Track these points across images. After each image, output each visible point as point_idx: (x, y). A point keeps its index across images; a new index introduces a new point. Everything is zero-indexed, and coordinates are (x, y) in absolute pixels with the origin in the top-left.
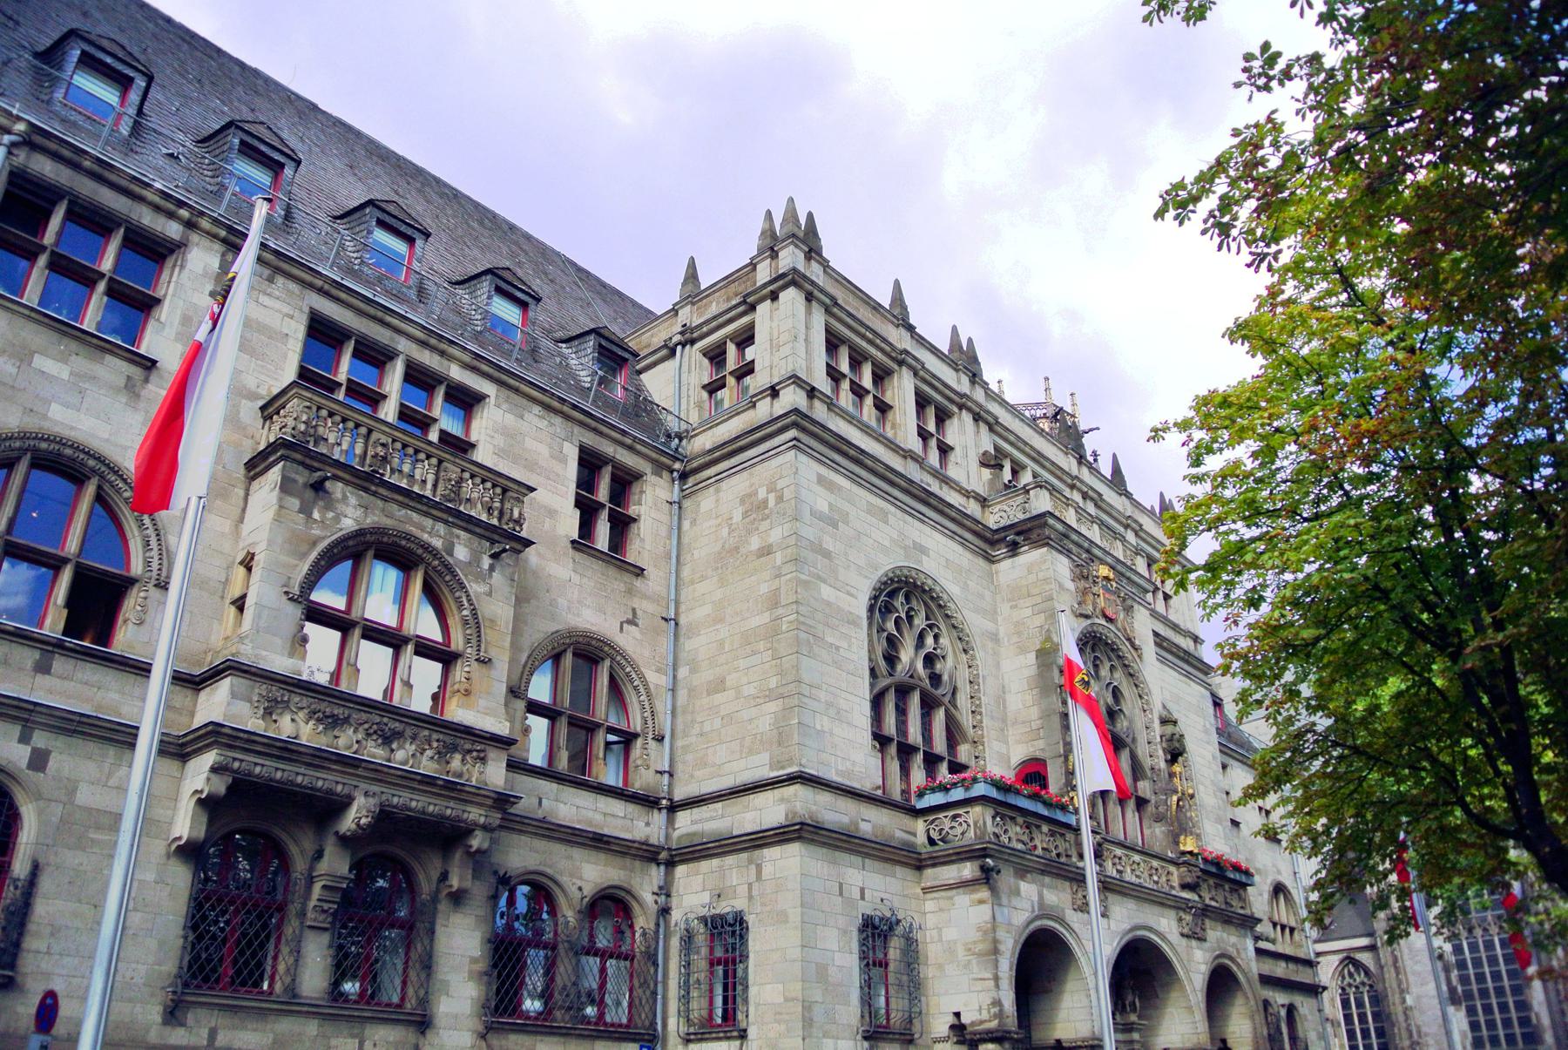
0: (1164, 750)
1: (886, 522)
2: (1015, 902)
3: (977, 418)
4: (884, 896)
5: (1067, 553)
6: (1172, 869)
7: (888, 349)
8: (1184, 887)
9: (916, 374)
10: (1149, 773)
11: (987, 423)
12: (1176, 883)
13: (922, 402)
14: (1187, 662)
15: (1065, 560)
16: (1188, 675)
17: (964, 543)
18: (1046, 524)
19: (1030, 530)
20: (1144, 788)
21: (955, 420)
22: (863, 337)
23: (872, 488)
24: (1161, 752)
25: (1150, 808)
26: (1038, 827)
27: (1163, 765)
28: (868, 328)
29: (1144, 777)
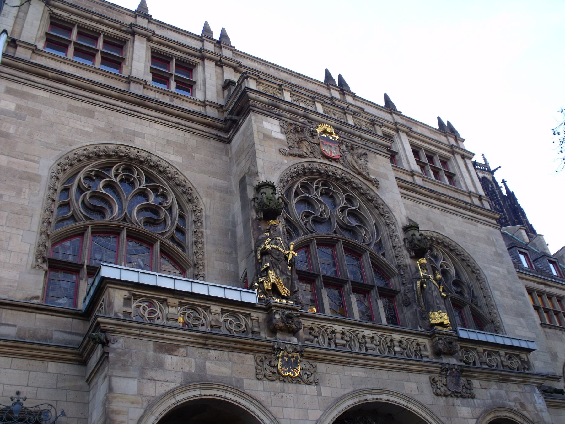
0: (408, 249)
1: (93, 117)
2: (158, 375)
3: (220, 64)
4: (18, 389)
5: (278, 117)
6: (421, 340)
7: (117, 25)
9: (149, 40)
10: (396, 270)
11: (231, 67)
12: (428, 352)
13: (158, 58)
14: (470, 210)
15: (277, 122)
16: (473, 219)
17: (190, 130)
18: (249, 98)
19: (242, 108)
20: (395, 283)
21: (199, 68)
22: (91, 19)
23: (74, 97)
24: (405, 252)
25: (399, 298)
26: (207, 308)
27: (409, 261)
28: (92, 13)
29: (393, 274)
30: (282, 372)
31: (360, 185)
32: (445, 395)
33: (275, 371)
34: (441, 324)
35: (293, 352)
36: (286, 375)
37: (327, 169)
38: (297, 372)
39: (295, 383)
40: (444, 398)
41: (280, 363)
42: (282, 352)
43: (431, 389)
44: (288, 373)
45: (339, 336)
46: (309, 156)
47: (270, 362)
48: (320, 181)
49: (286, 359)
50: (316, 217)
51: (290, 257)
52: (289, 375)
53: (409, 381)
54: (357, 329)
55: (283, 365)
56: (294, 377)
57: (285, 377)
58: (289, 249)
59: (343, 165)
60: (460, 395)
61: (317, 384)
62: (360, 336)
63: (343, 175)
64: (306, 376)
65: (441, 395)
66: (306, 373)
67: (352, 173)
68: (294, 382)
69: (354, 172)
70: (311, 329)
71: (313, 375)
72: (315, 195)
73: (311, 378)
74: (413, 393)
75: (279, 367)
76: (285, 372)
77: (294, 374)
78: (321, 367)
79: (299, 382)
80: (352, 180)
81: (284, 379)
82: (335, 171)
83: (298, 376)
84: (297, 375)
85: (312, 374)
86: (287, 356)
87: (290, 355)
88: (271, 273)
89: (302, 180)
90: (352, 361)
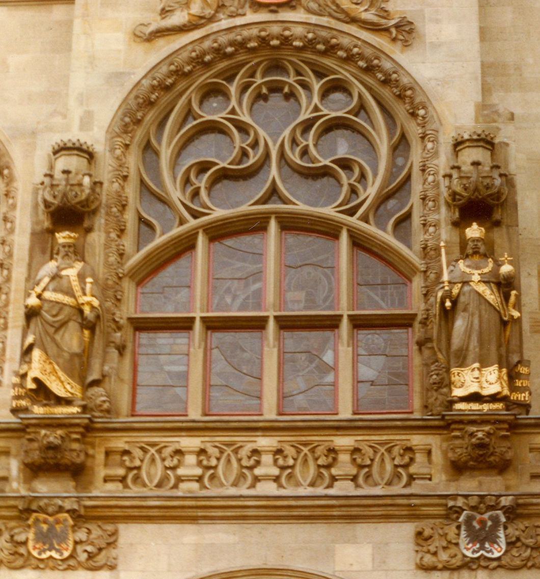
6: (417, 440)
8: (458, 468)
30: (35, 553)
31: (356, 50)
32: (445, 568)
33: (22, 550)
34: (475, 397)
35: (57, 512)
36: (44, 556)
37: (263, 34)
38: (67, 549)
39: (65, 569)
40: (446, 574)
41: (31, 535)
42: (35, 515)
43: (414, 554)
44: (48, 554)
45: (191, 459)
46: (211, 19)
47: (12, 536)
48: (258, 64)
49: (45, 527)
50: (224, 169)
51: (87, 310)
52: (51, 557)
53: (353, 540)
54: (238, 438)
55: (37, 540)
56: (62, 560)
57: (42, 560)
58: (85, 294)
59: (309, 11)
60: (495, 564)
61: (112, 568)
62: (244, 453)
63: (310, 36)
64: (85, 555)
65: (434, 568)
66: (86, 551)
67: (334, 23)
68: (61, 568)
69: (338, 19)
70: (126, 452)
71: (104, 553)
72: (233, 111)
73: (101, 559)
74: (355, 568)
75: (31, 544)
76: (44, 551)
77: (62, 554)
78: (129, 533)
79: (70, 568)
80: (334, 41)
81: (41, 565)
82: (287, 33)
83: (71, 556)
84: (66, 554)
85: (100, 550)
86: (45, 522)
87: (51, 519)
88: (36, 353)
89: (204, 78)
90: (200, 514)
